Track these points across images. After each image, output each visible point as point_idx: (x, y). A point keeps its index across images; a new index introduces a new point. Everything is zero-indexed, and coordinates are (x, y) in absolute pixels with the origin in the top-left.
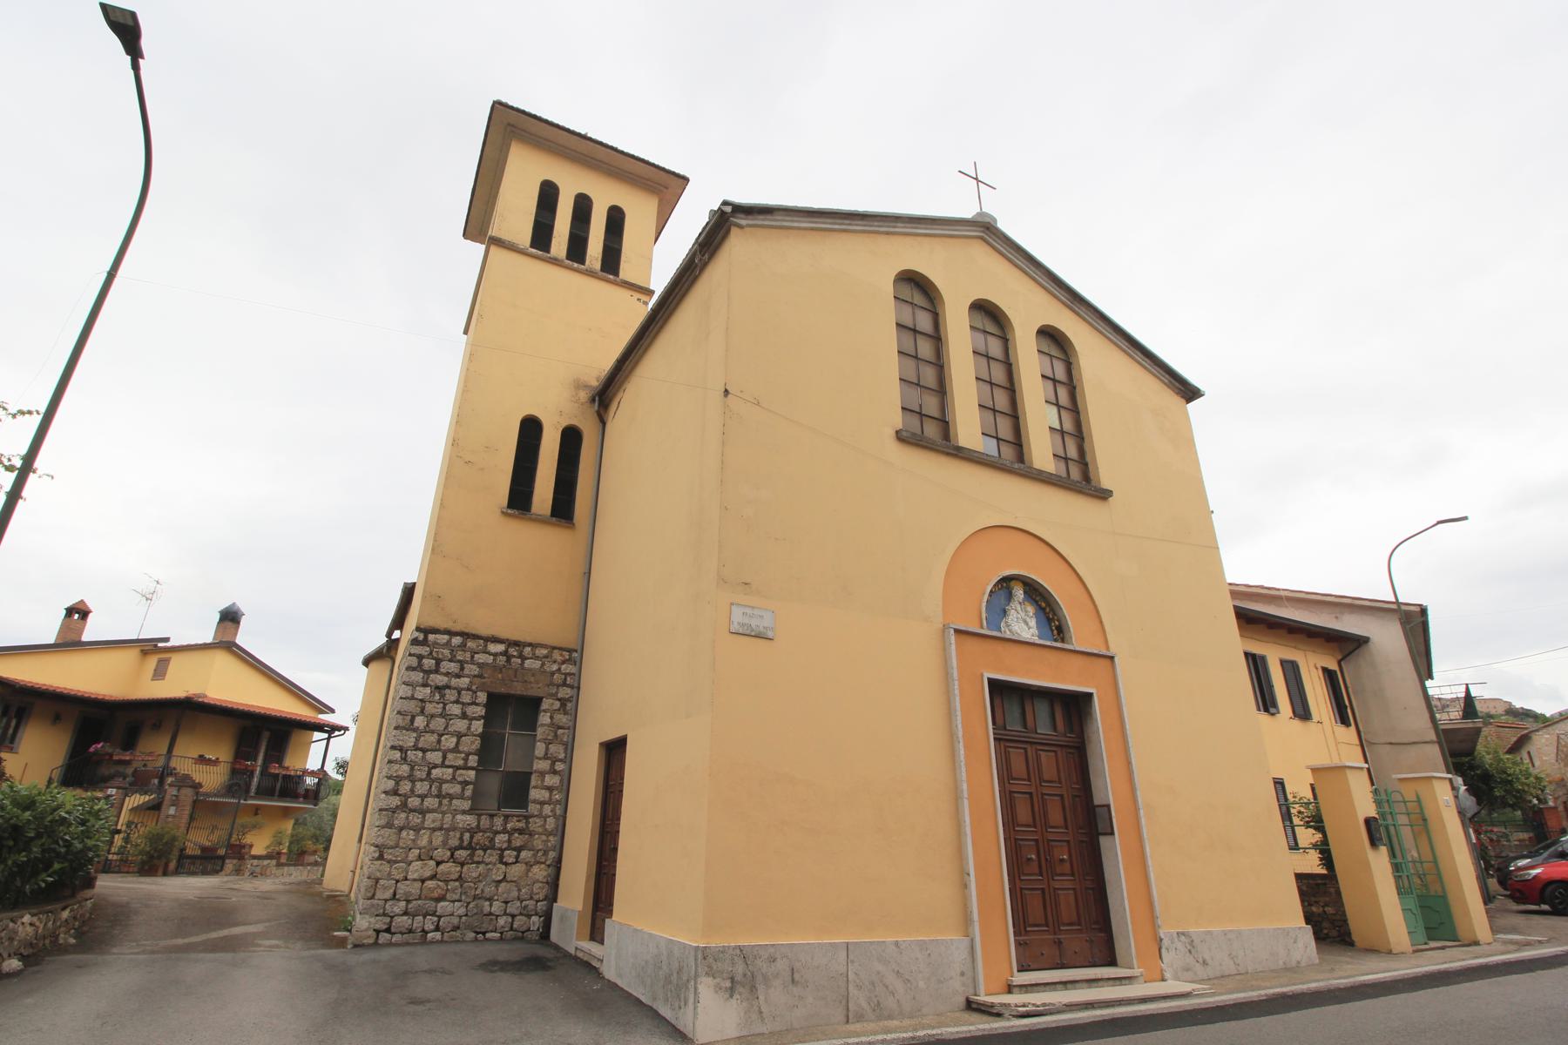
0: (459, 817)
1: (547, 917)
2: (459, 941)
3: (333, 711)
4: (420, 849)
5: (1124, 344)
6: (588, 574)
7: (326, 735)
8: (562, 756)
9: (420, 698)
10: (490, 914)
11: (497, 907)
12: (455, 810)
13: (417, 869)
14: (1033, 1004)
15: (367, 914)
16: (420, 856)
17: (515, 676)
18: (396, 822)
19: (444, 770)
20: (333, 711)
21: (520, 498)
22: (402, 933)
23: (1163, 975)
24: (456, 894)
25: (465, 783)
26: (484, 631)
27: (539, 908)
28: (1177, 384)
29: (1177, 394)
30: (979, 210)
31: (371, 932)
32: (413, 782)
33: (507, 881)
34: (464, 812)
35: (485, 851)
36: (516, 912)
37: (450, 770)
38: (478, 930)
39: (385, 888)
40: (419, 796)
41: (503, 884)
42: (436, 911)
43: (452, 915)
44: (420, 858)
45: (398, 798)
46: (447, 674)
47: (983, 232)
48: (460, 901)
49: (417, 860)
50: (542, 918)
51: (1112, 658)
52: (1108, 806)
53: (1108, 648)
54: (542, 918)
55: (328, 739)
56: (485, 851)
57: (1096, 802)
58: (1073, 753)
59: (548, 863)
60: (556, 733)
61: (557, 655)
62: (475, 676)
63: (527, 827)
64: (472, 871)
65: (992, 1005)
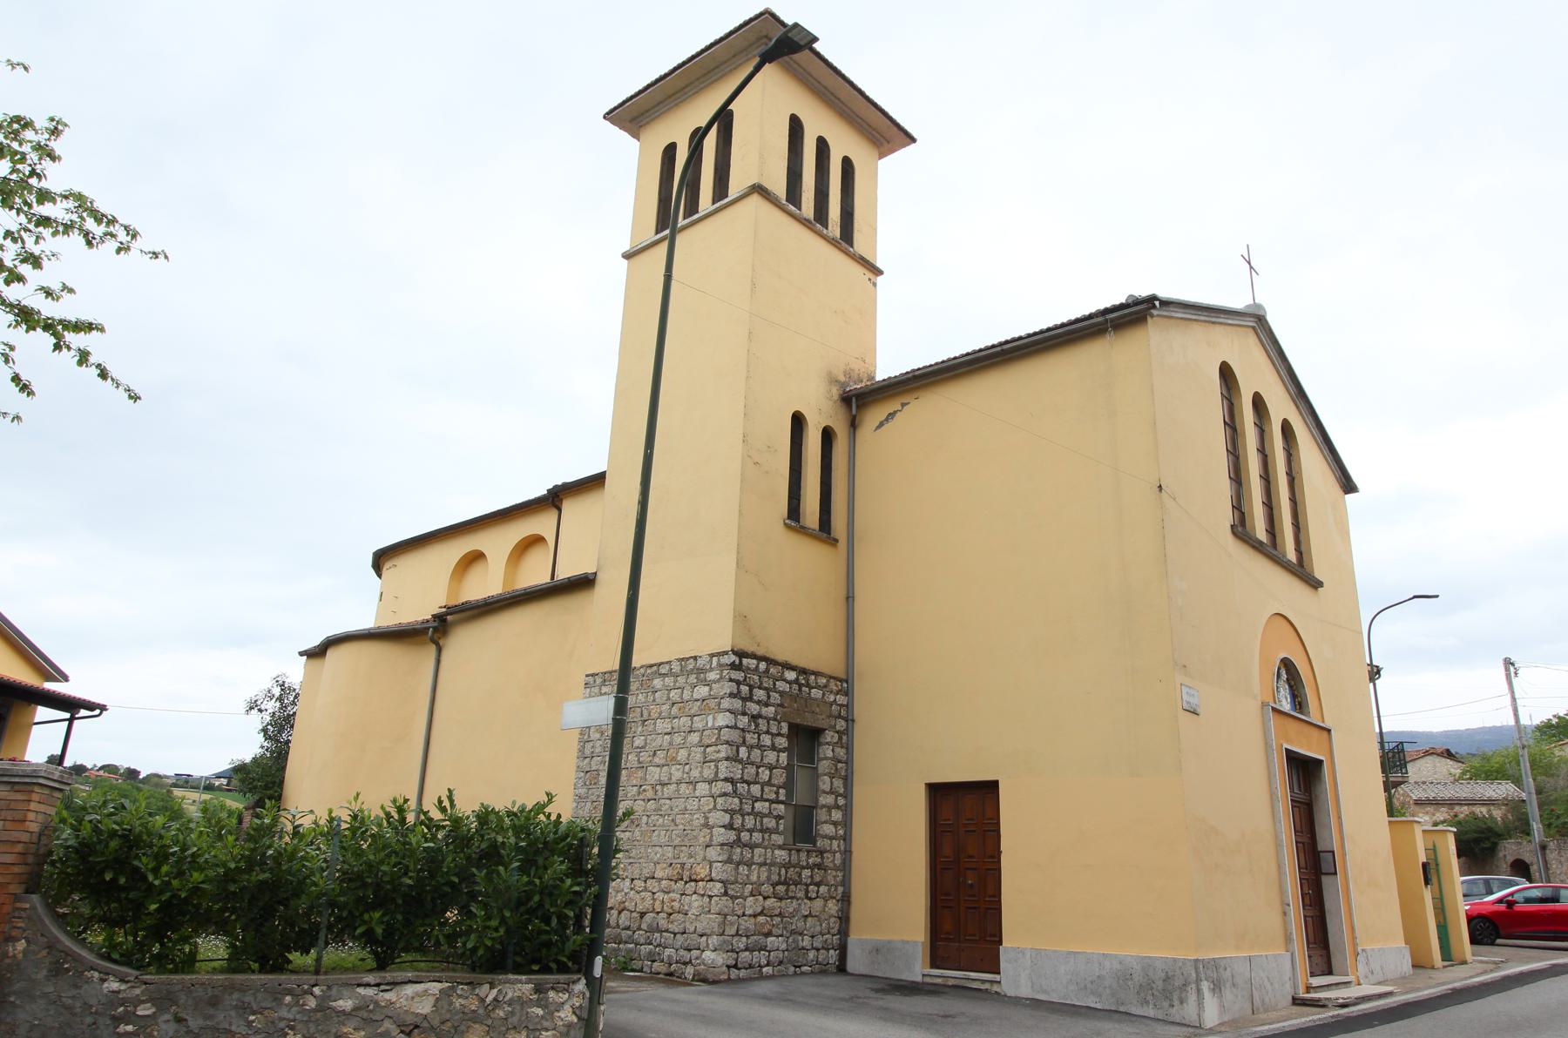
0: (777, 852)
1: (843, 950)
2: (784, 975)
3: (66, 678)
4: (752, 884)
5: (1319, 439)
6: (850, 598)
7: (67, 715)
8: (842, 791)
9: (741, 727)
10: (803, 948)
11: (806, 942)
12: (773, 845)
13: (752, 905)
14: (1342, 998)
15: (720, 950)
16: (751, 892)
17: (806, 706)
18: (734, 857)
19: (763, 803)
20: (66, 678)
21: (794, 511)
22: (746, 969)
23: (1359, 981)
24: (779, 929)
25: (779, 818)
26: (780, 658)
27: (835, 942)
28: (1343, 480)
29: (1341, 487)
30: (1252, 302)
31: (725, 968)
32: (743, 815)
33: (812, 916)
34: (780, 847)
35: (796, 885)
36: (820, 946)
37: (767, 803)
38: (796, 964)
39: (732, 924)
40: (748, 830)
41: (810, 919)
42: (766, 946)
43: (778, 950)
44: (752, 895)
45: (734, 832)
46: (758, 702)
47: (1256, 322)
48: (782, 936)
49: (750, 896)
50: (838, 951)
51: (1329, 731)
52: (1333, 852)
53: (1323, 722)
54: (838, 951)
55: (71, 721)
56: (796, 885)
57: (1319, 849)
58: (1298, 807)
59: (838, 898)
60: (836, 766)
61: (833, 686)
62: (778, 705)
63: (823, 863)
64: (790, 906)
65: (1319, 1000)
